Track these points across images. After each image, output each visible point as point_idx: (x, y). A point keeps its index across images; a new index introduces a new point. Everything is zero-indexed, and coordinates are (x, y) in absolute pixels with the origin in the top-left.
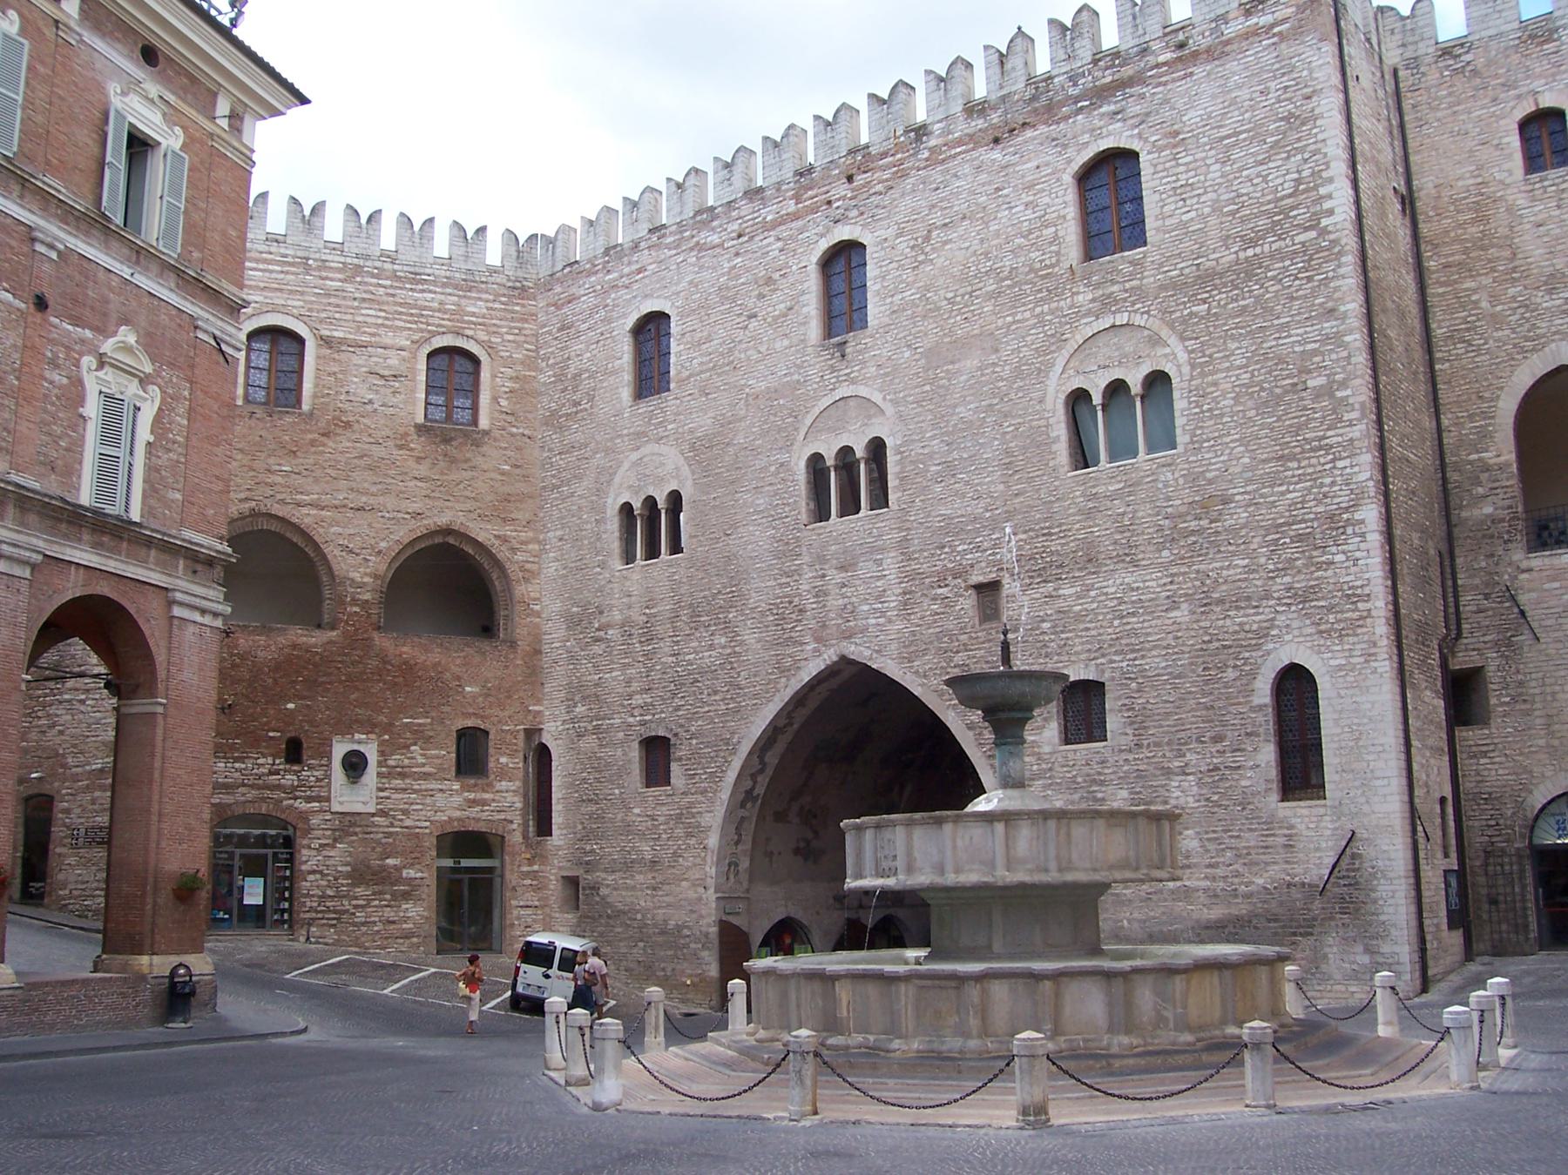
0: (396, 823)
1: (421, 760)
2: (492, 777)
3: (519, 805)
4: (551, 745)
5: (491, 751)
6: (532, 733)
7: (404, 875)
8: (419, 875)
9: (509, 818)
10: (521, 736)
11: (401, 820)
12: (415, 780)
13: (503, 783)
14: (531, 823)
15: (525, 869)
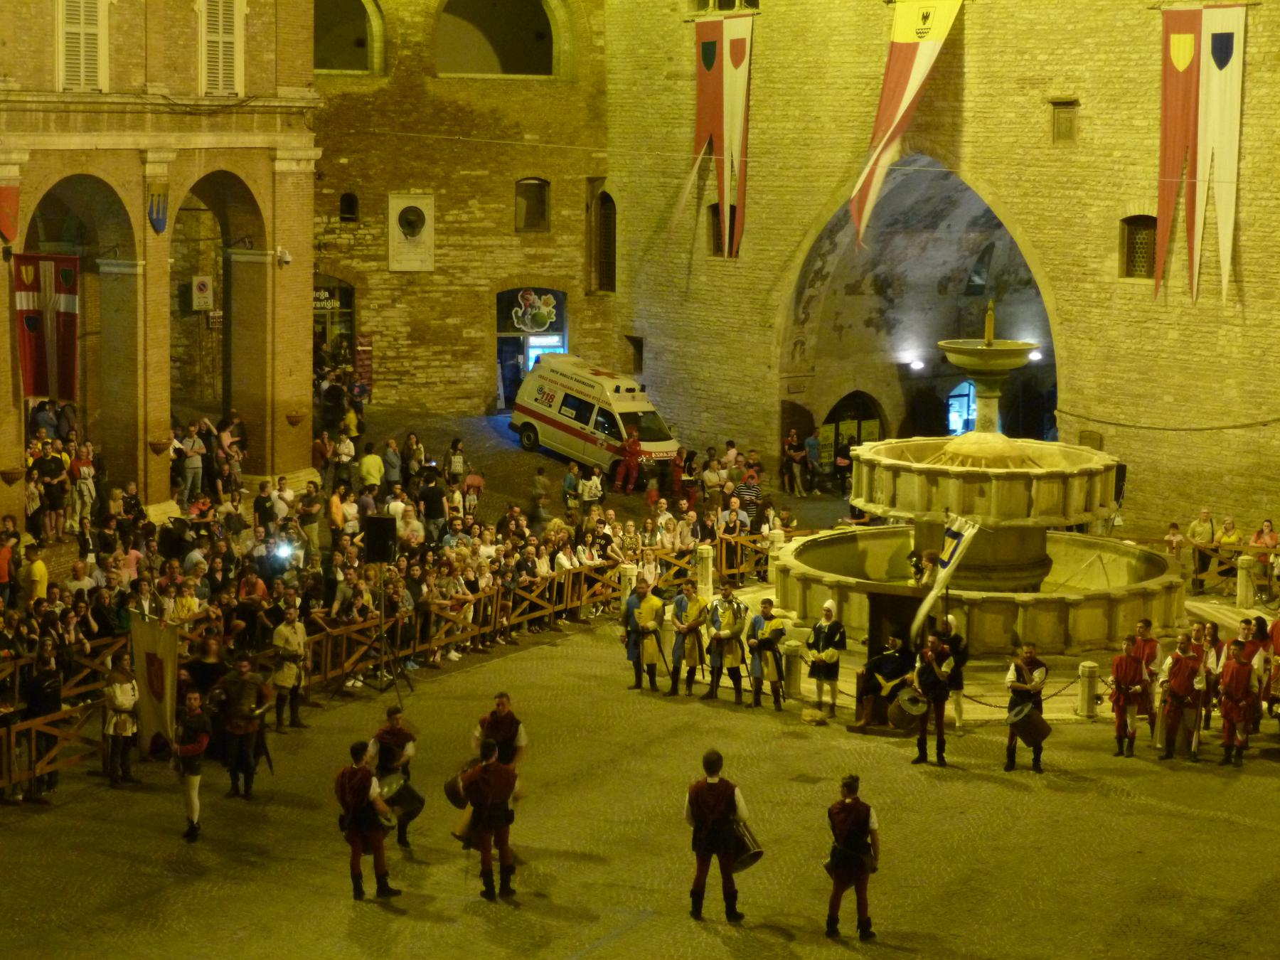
0: (456, 281)
1: (479, 214)
2: (553, 230)
3: (581, 260)
4: (615, 196)
5: (553, 202)
6: (595, 181)
7: (465, 335)
8: (480, 334)
9: (571, 273)
10: (583, 186)
11: (460, 278)
12: (473, 235)
13: (565, 237)
14: (593, 275)
15: (587, 326)
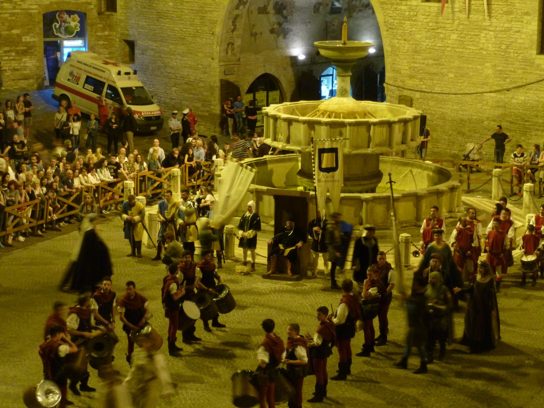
0: (17, 7)
7: (23, 40)
8: (33, 40)
11: (20, 5)
15: (99, 34)
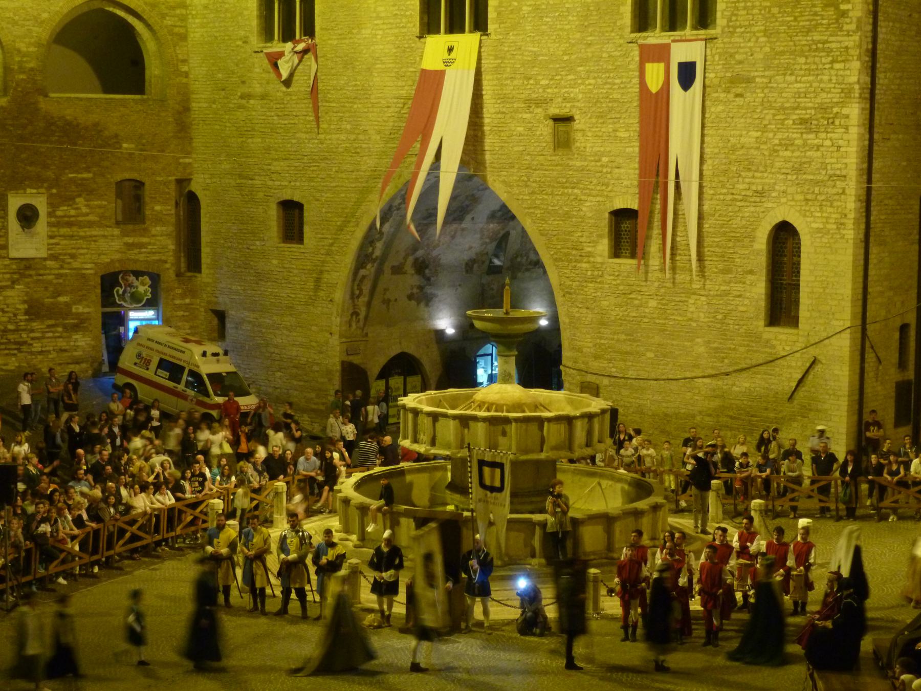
0: (66, 266)
1: (85, 210)
2: (148, 223)
3: (172, 247)
4: (200, 194)
5: (147, 199)
6: (182, 182)
7: (74, 310)
8: (86, 310)
9: (163, 258)
10: (173, 186)
11: (69, 263)
12: (80, 227)
13: (158, 228)
14: (183, 260)
15: (177, 302)
